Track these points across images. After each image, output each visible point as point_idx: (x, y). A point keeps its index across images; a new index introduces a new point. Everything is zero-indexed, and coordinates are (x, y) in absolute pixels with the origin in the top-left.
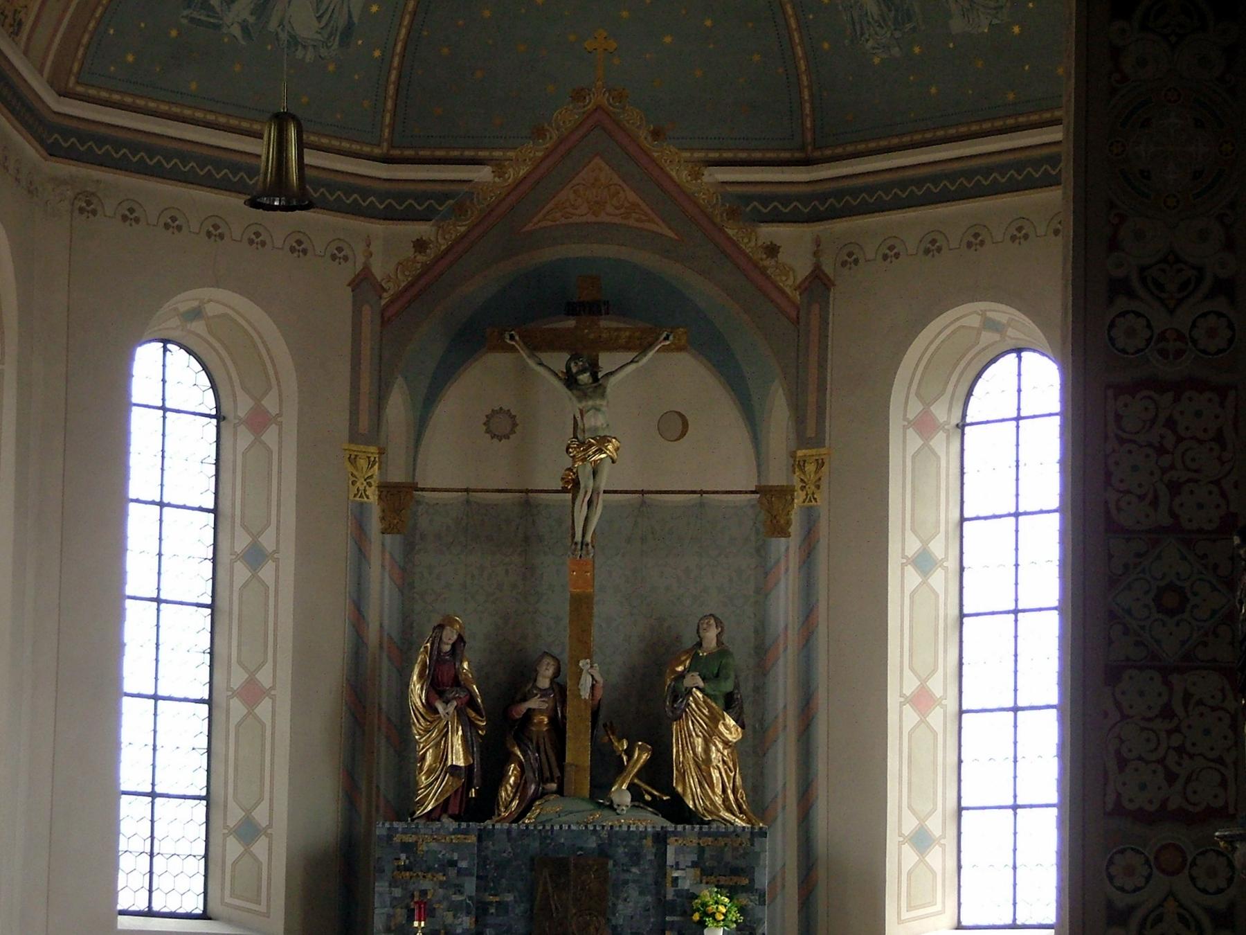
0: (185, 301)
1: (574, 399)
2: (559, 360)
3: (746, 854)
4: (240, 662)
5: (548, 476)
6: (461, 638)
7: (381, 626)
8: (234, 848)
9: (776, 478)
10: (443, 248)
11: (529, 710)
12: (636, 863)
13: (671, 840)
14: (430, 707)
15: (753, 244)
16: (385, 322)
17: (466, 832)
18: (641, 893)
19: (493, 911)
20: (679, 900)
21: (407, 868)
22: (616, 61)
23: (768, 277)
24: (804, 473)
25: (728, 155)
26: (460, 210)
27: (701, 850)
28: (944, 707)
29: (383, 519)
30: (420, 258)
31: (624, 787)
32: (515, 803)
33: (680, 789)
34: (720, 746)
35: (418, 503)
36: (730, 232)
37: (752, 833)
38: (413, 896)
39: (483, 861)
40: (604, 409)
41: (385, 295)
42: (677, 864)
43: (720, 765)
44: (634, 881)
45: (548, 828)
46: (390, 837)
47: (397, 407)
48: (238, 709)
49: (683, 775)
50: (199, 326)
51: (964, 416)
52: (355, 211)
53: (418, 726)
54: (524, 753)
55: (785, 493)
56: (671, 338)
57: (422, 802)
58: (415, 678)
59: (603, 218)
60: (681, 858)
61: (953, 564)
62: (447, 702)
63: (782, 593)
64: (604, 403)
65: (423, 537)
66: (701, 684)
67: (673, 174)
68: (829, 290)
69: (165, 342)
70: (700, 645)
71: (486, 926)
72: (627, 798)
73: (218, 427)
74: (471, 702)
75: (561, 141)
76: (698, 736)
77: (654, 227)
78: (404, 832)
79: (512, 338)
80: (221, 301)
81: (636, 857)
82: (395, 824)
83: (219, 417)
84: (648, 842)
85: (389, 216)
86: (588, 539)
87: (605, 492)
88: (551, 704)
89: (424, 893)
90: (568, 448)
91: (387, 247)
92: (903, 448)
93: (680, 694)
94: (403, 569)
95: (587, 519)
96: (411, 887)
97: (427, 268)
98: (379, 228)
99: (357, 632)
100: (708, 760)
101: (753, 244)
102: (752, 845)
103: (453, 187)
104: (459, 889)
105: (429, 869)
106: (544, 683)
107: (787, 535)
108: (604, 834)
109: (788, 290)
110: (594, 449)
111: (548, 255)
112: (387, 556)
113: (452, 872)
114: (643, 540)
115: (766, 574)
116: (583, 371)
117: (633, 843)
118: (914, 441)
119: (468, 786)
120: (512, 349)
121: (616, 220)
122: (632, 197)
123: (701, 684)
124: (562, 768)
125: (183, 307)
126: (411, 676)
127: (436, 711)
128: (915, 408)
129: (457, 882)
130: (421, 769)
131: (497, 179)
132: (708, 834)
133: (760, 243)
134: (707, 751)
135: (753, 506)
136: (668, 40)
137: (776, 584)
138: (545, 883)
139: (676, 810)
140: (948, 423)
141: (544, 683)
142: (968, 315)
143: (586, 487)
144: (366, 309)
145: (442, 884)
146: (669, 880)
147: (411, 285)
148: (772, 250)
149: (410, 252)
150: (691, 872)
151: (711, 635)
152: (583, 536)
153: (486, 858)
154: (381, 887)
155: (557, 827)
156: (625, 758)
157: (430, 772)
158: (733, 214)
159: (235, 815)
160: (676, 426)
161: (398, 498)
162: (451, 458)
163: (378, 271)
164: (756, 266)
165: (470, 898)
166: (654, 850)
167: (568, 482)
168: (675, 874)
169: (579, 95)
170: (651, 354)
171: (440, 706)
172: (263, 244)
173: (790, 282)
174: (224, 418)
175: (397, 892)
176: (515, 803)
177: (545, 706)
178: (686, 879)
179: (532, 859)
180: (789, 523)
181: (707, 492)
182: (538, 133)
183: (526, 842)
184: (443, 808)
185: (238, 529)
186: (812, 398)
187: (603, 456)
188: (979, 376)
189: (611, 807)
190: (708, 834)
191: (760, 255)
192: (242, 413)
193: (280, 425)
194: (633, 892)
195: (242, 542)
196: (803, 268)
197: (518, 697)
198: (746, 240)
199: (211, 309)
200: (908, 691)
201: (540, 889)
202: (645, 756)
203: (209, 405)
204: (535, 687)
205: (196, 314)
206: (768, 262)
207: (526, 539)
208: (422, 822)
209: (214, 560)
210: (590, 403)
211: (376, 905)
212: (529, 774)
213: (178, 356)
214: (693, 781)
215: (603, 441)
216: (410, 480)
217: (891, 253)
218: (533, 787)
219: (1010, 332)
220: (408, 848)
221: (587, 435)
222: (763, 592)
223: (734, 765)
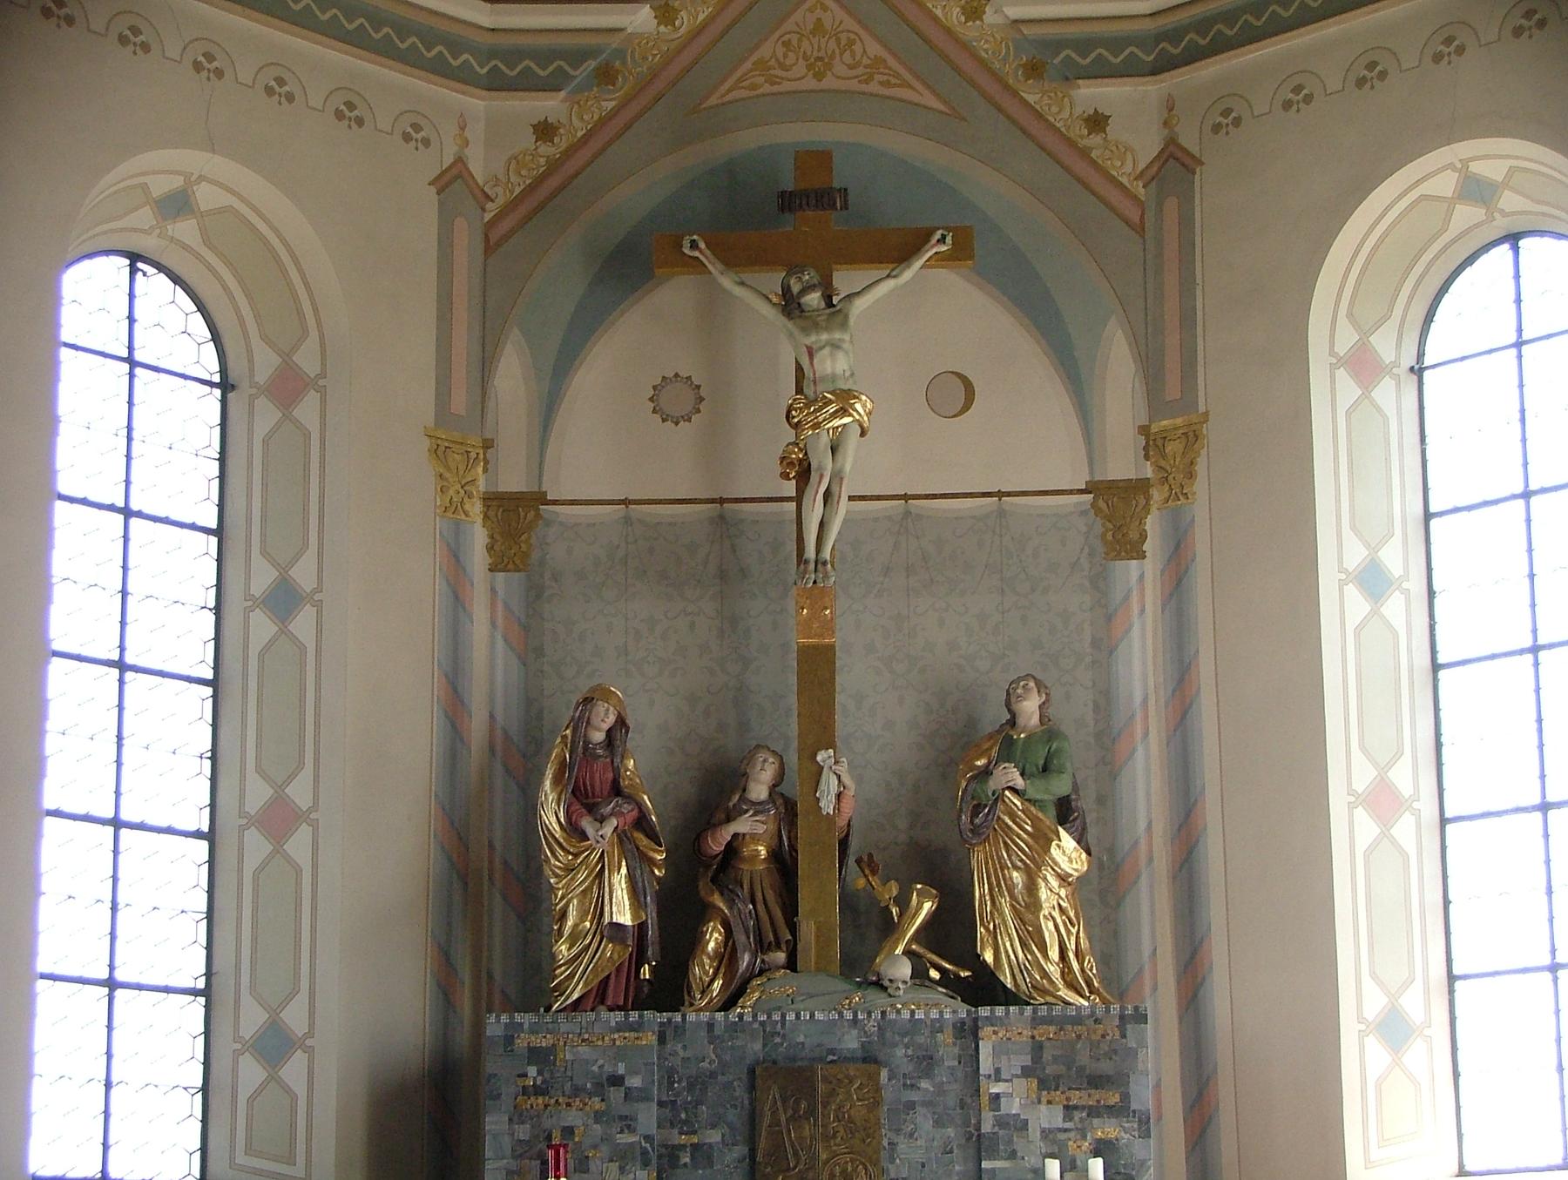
0: (161, 167)
1: (796, 332)
2: (772, 280)
3: (1115, 1052)
4: (259, 770)
5: (758, 473)
6: (621, 722)
7: (492, 716)
8: (252, 1072)
9: (1124, 463)
10: (580, 134)
11: (735, 836)
12: (928, 1073)
13: (986, 1031)
14: (574, 831)
15: (1065, 114)
16: (489, 249)
17: (637, 1027)
18: (938, 1123)
19: (686, 1159)
20: (1001, 1132)
21: (538, 1091)
23: (1093, 163)
24: (1164, 456)
26: (606, 75)
27: (1037, 1048)
28: (1417, 814)
29: (490, 548)
30: (545, 149)
31: (899, 951)
32: (718, 984)
33: (989, 957)
34: (1054, 883)
35: (548, 524)
36: (1031, 98)
37: (1122, 1017)
38: (549, 1138)
39: (670, 1077)
40: (846, 346)
41: (489, 205)
42: (998, 1071)
43: (1056, 914)
44: (927, 1104)
45: (776, 1017)
46: (509, 1040)
47: (512, 376)
48: (257, 846)
50: (186, 229)
51: (1421, 355)
52: (440, 69)
53: (556, 861)
54: (731, 903)
55: (1139, 487)
56: (949, 239)
57: (560, 989)
58: (547, 784)
59: (829, 82)
60: (1004, 1064)
61: (1417, 586)
62: (602, 820)
63: (1136, 645)
64: (847, 337)
65: (556, 577)
66: (1019, 782)
67: (939, 12)
68: (1194, 173)
69: (134, 258)
70: (1012, 722)
72: (905, 970)
73: (224, 401)
74: (642, 822)
76: (1016, 868)
77: (916, 98)
78: (534, 1030)
79: (694, 245)
80: (222, 180)
81: (926, 1062)
82: (518, 1018)
83: (226, 385)
84: (946, 1038)
85: (496, 84)
86: (827, 554)
88: (772, 827)
89: (569, 1131)
90: (789, 412)
91: (490, 132)
92: (1331, 399)
94: (526, 629)
95: (822, 525)
96: (547, 1123)
97: (553, 166)
98: (477, 104)
99: (453, 725)
100: (1034, 905)
101: (1065, 114)
102: (1124, 1036)
103: (592, 40)
104: (628, 1123)
105: (577, 1091)
106: (759, 791)
107: (1142, 556)
108: (872, 1027)
109: (1124, 180)
110: (832, 408)
111: (748, 140)
112: (500, 607)
113: (616, 1095)
114: (909, 570)
115: (1109, 619)
116: (806, 290)
117: (921, 1040)
118: (1348, 389)
119: (640, 958)
120: (696, 265)
121: (854, 85)
122: (874, 49)
123: (1019, 782)
124: (793, 928)
125: (162, 186)
126: (540, 783)
127: (584, 836)
128: (1346, 339)
129: (625, 1111)
130: (560, 933)
131: (662, 28)
132: (1048, 1020)
133: (1078, 111)
134: (1031, 888)
135: (1083, 513)
137: (1128, 631)
139: (983, 988)
140: (1396, 364)
141: (759, 791)
142: (1431, 174)
143: (820, 468)
144: (460, 224)
145: (598, 1116)
146: (985, 1100)
147: (531, 189)
148: (1097, 122)
149: (527, 140)
150: (1021, 1084)
151: (1030, 708)
152: (818, 550)
153: (671, 1072)
154: (495, 1123)
155: (791, 1016)
156: (894, 911)
157: (573, 939)
158: (1034, 70)
159: (253, 1019)
161: (516, 517)
162: (602, 449)
163: (477, 168)
164: (1071, 143)
165: (648, 1138)
166: (956, 1050)
167: (791, 464)
168: (994, 1090)
171: (587, 824)
172: (290, 98)
173: (1128, 168)
174: (233, 387)
175: (523, 1131)
176: (718, 984)
177: (761, 829)
178: (1014, 1096)
179: (752, 1071)
180: (1143, 537)
181: (1009, 494)
183: (739, 1043)
184: (599, 995)
185: (257, 559)
186: (1172, 340)
187: (847, 420)
188: (1470, 260)
189: (879, 985)
190: (1048, 1020)
191: (1078, 131)
192: (262, 377)
193: (322, 391)
194: (924, 1121)
195: (263, 578)
196: (1147, 147)
198: (1054, 109)
199: (207, 197)
200: (1360, 786)
201: (767, 1121)
202: (927, 906)
203: (209, 364)
204: (743, 799)
205: (177, 205)
206: (1096, 140)
207: (722, 575)
208: (561, 1017)
209: (218, 610)
210: (824, 337)
211: (488, 1154)
212: (740, 938)
213: (155, 285)
214: (1011, 946)
215: (845, 400)
216: (536, 489)
217: (1298, 96)
218: (747, 957)
219: (1509, 201)
220: (538, 1056)
221: (820, 389)
222: (1105, 648)
223: (1077, 915)
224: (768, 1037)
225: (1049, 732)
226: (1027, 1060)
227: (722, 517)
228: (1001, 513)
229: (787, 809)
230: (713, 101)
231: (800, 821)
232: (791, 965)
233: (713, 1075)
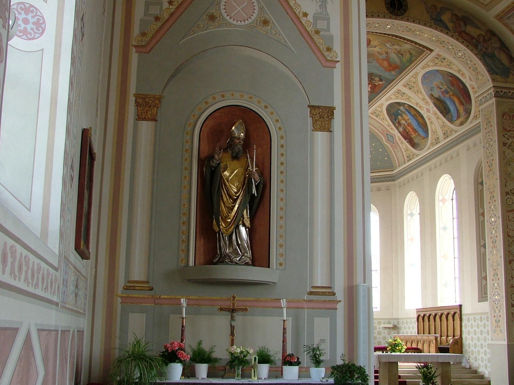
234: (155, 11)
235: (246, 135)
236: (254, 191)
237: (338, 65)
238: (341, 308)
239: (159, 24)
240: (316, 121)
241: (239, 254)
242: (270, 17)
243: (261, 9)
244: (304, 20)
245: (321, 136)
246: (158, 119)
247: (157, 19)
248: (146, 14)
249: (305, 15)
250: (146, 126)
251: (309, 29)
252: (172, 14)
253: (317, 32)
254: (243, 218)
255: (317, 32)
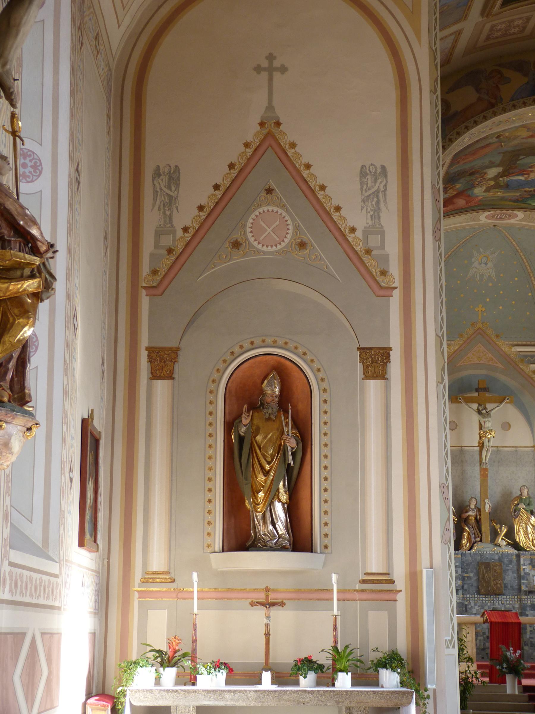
2: (475, 406)
11: (469, 516)
12: (511, 564)
13: (522, 556)
18: (513, 573)
19: (466, 579)
22: (485, 314)
25: (520, 343)
27: (531, 560)
32: (468, 544)
33: (518, 540)
36: (521, 366)
44: (511, 570)
49: (519, 535)
54: (469, 529)
59: (482, 362)
66: (524, 507)
67: (503, 348)
70: (521, 494)
71: (465, 584)
75: (468, 338)
81: (510, 562)
84: (514, 557)
86: (487, 461)
87: (492, 447)
93: (517, 510)
106: (473, 507)
108: (500, 555)
114: (499, 462)
116: (483, 409)
120: (460, 402)
121: (486, 363)
122: (490, 355)
123: (524, 507)
134: (526, 528)
135: (533, 451)
136: (501, 308)
138: (483, 570)
139: (516, 546)
141: (473, 507)
146: (522, 569)
151: (525, 491)
153: (463, 562)
156: (499, 530)
158: (522, 361)
160: (506, 426)
164: (529, 376)
168: (524, 567)
169: (473, 325)
170: (503, 404)
176: (468, 544)
177: (474, 514)
182: (461, 336)
194: (510, 573)
197: (464, 511)
204: (470, 508)
212: (472, 535)
224: (481, 556)
225: (529, 497)
226: (530, 562)
227: (462, 450)
228: (516, 451)
229: (479, 510)
230: (459, 365)
231: (482, 513)
232: (481, 541)
233: (471, 563)
234: (167, 241)
235: (281, 391)
236: (290, 461)
237: (396, 293)
238: (402, 599)
239: (173, 258)
240: (368, 366)
241: (276, 536)
242: (308, 237)
243: (297, 228)
244: (351, 237)
245: (374, 386)
246: (175, 375)
247: (170, 251)
248: (157, 246)
249: (353, 230)
250: (161, 386)
251: (358, 249)
252: (188, 244)
253: (368, 252)
254: (279, 493)
255: (368, 252)
